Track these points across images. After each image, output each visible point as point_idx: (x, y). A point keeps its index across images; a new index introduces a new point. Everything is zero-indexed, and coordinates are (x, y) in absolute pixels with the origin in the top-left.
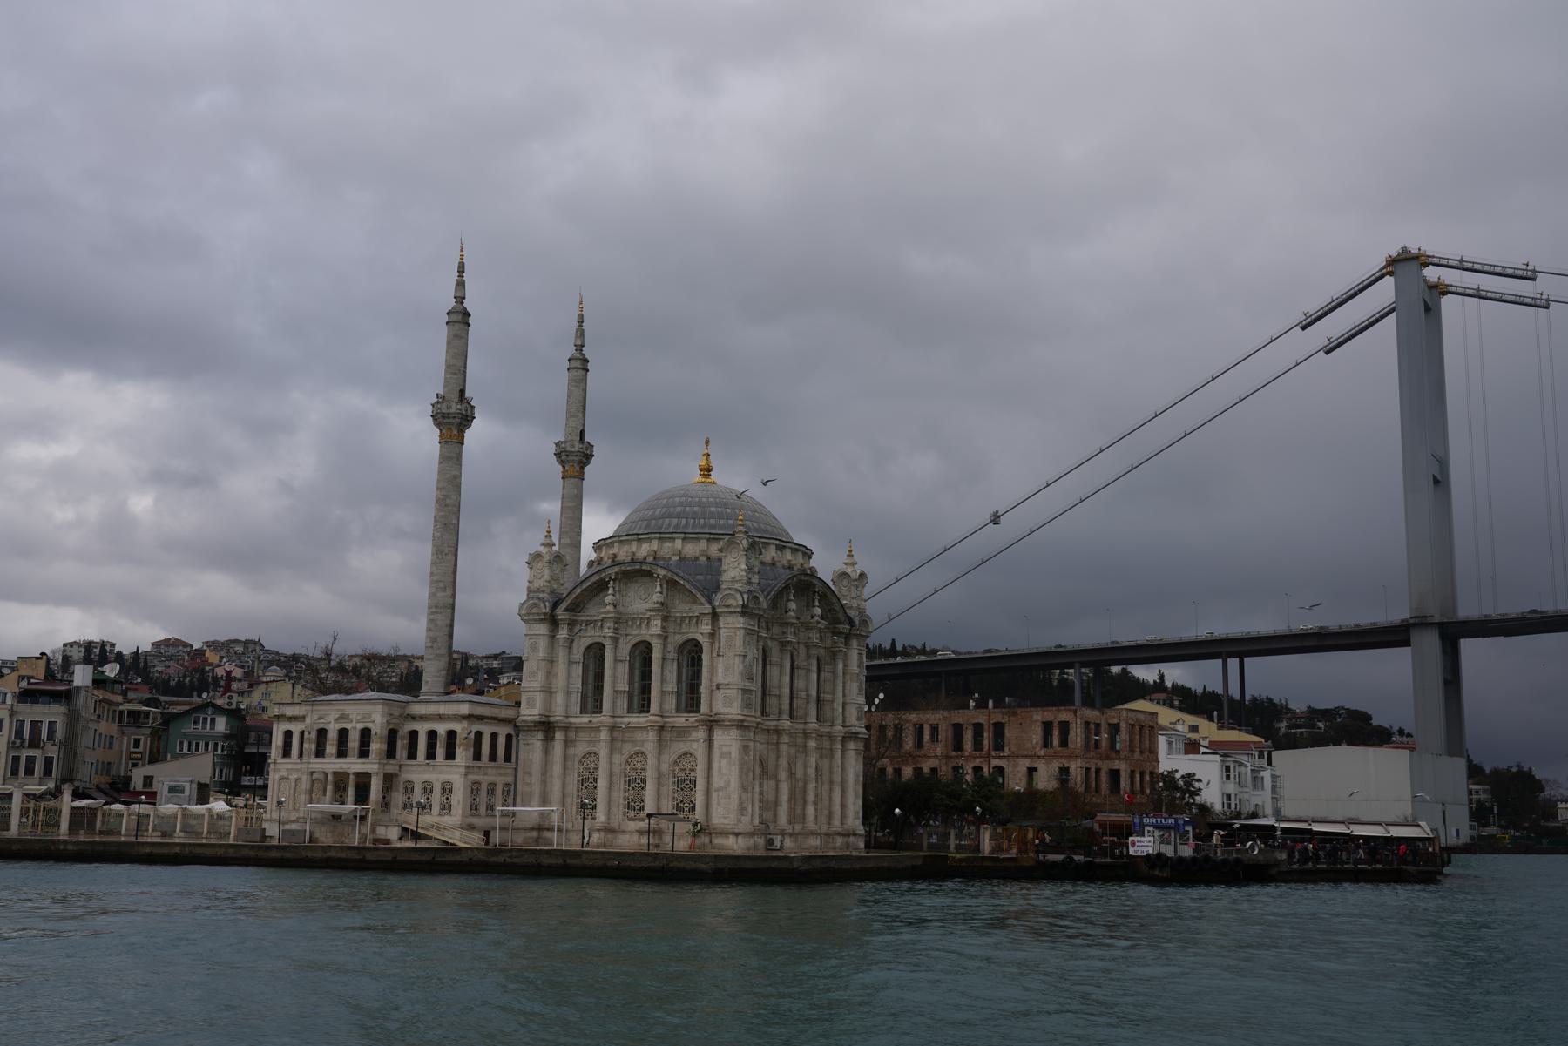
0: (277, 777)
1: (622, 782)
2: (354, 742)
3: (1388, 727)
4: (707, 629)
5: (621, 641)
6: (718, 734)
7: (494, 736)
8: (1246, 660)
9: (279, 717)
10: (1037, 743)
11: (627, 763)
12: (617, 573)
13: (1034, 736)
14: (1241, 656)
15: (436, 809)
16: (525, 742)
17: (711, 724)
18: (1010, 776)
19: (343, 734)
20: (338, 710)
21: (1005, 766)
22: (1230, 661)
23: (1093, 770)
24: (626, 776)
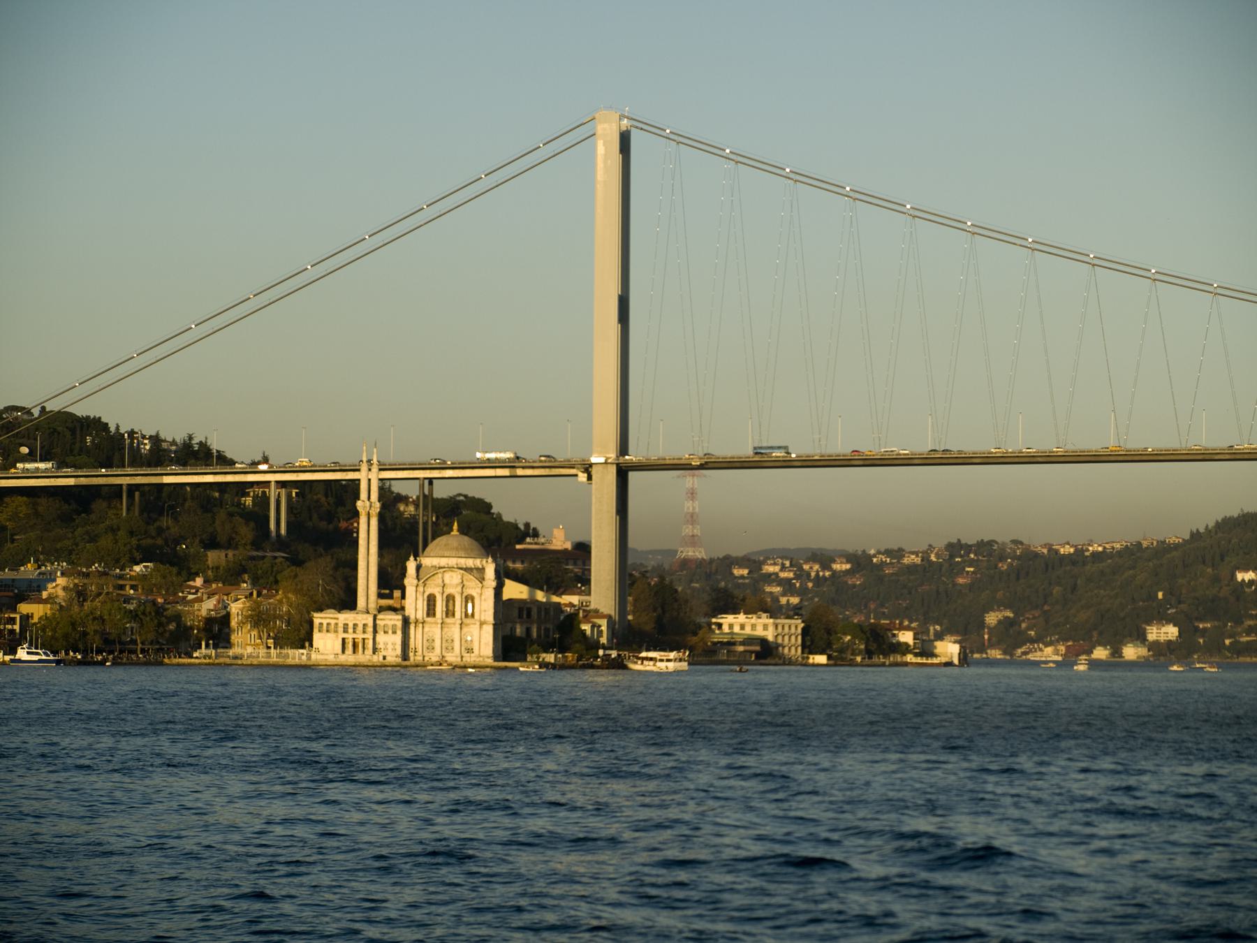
2: (360, 628)
3: (513, 521)
4: (479, 590)
6: (484, 626)
15: (390, 650)
17: (482, 624)
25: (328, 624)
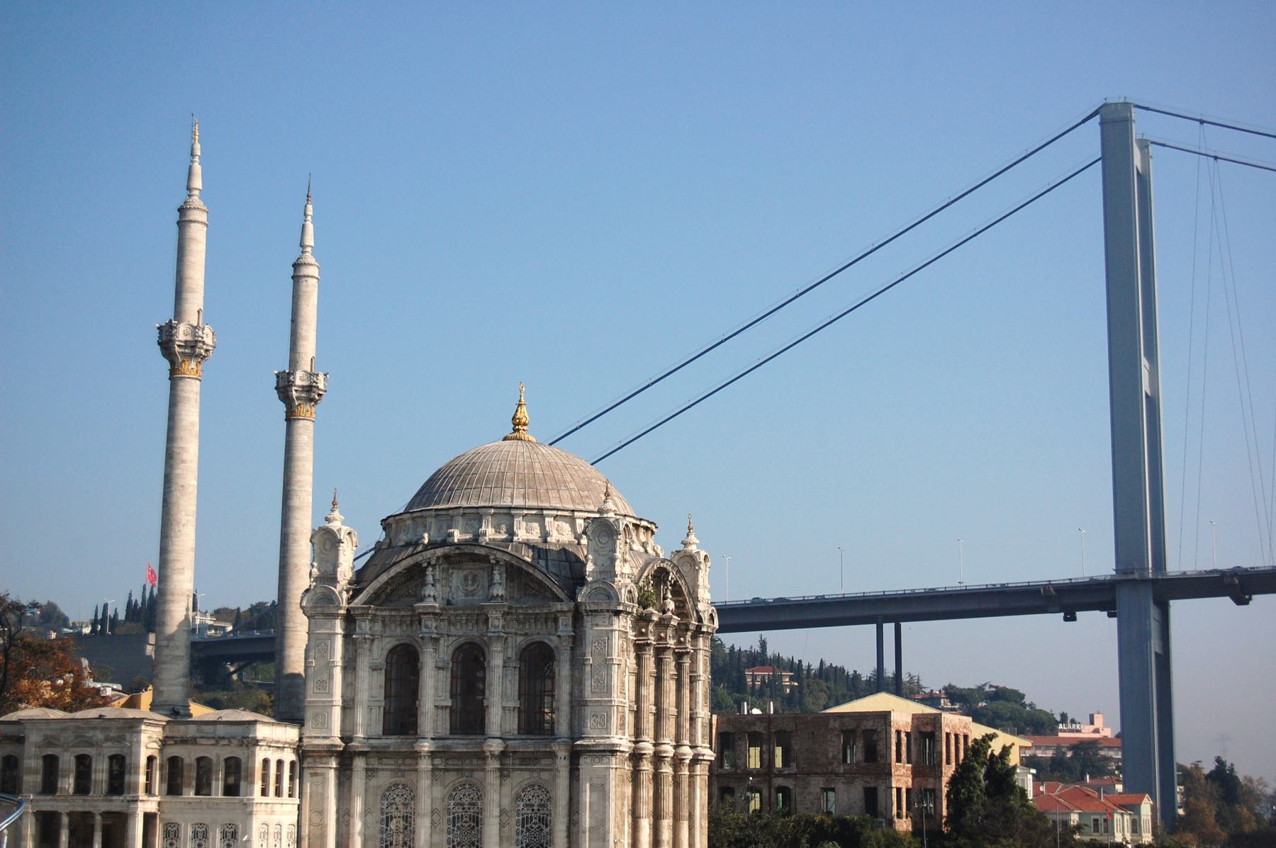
1: (446, 821)
2: (100, 773)
3: (1049, 711)
5: (442, 642)
7: (280, 763)
8: (903, 625)
10: (834, 757)
11: (451, 797)
12: (438, 558)
13: (830, 749)
14: (897, 620)
16: (311, 771)
18: (798, 799)
19: (83, 764)
21: (791, 787)
22: (885, 625)
23: (904, 790)
24: (449, 814)
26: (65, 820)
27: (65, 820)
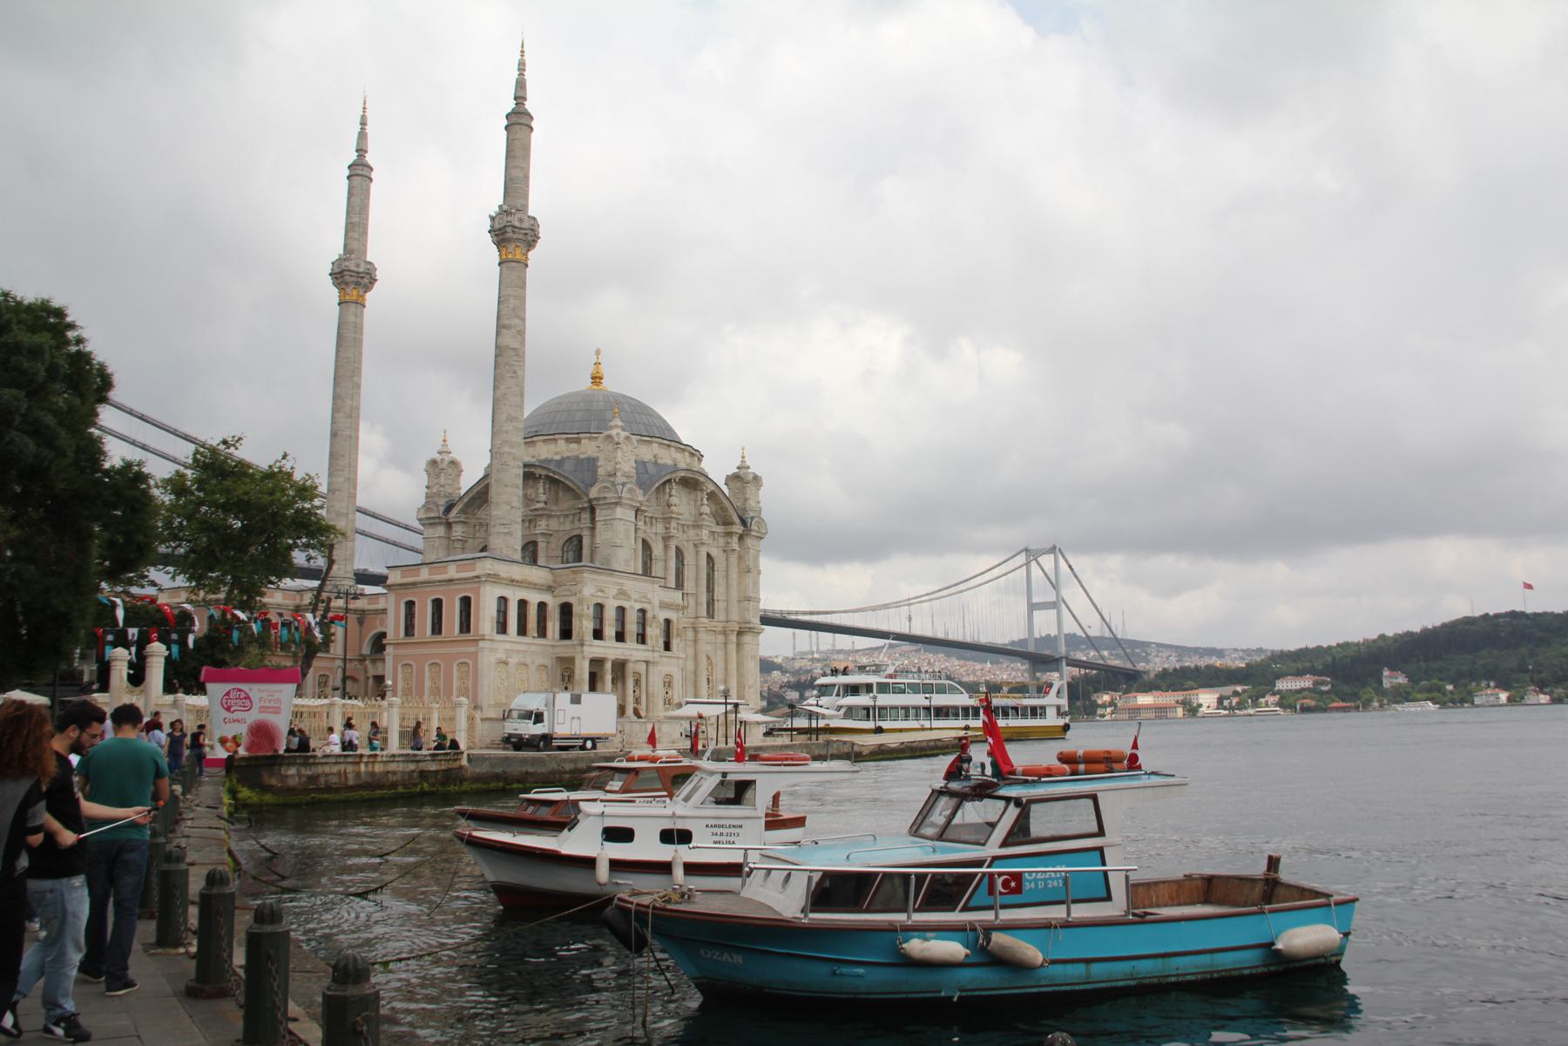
0: (493, 659)
9: (494, 578)
20: (617, 584)
25: (542, 606)
26: (608, 666)
27: (608, 666)
